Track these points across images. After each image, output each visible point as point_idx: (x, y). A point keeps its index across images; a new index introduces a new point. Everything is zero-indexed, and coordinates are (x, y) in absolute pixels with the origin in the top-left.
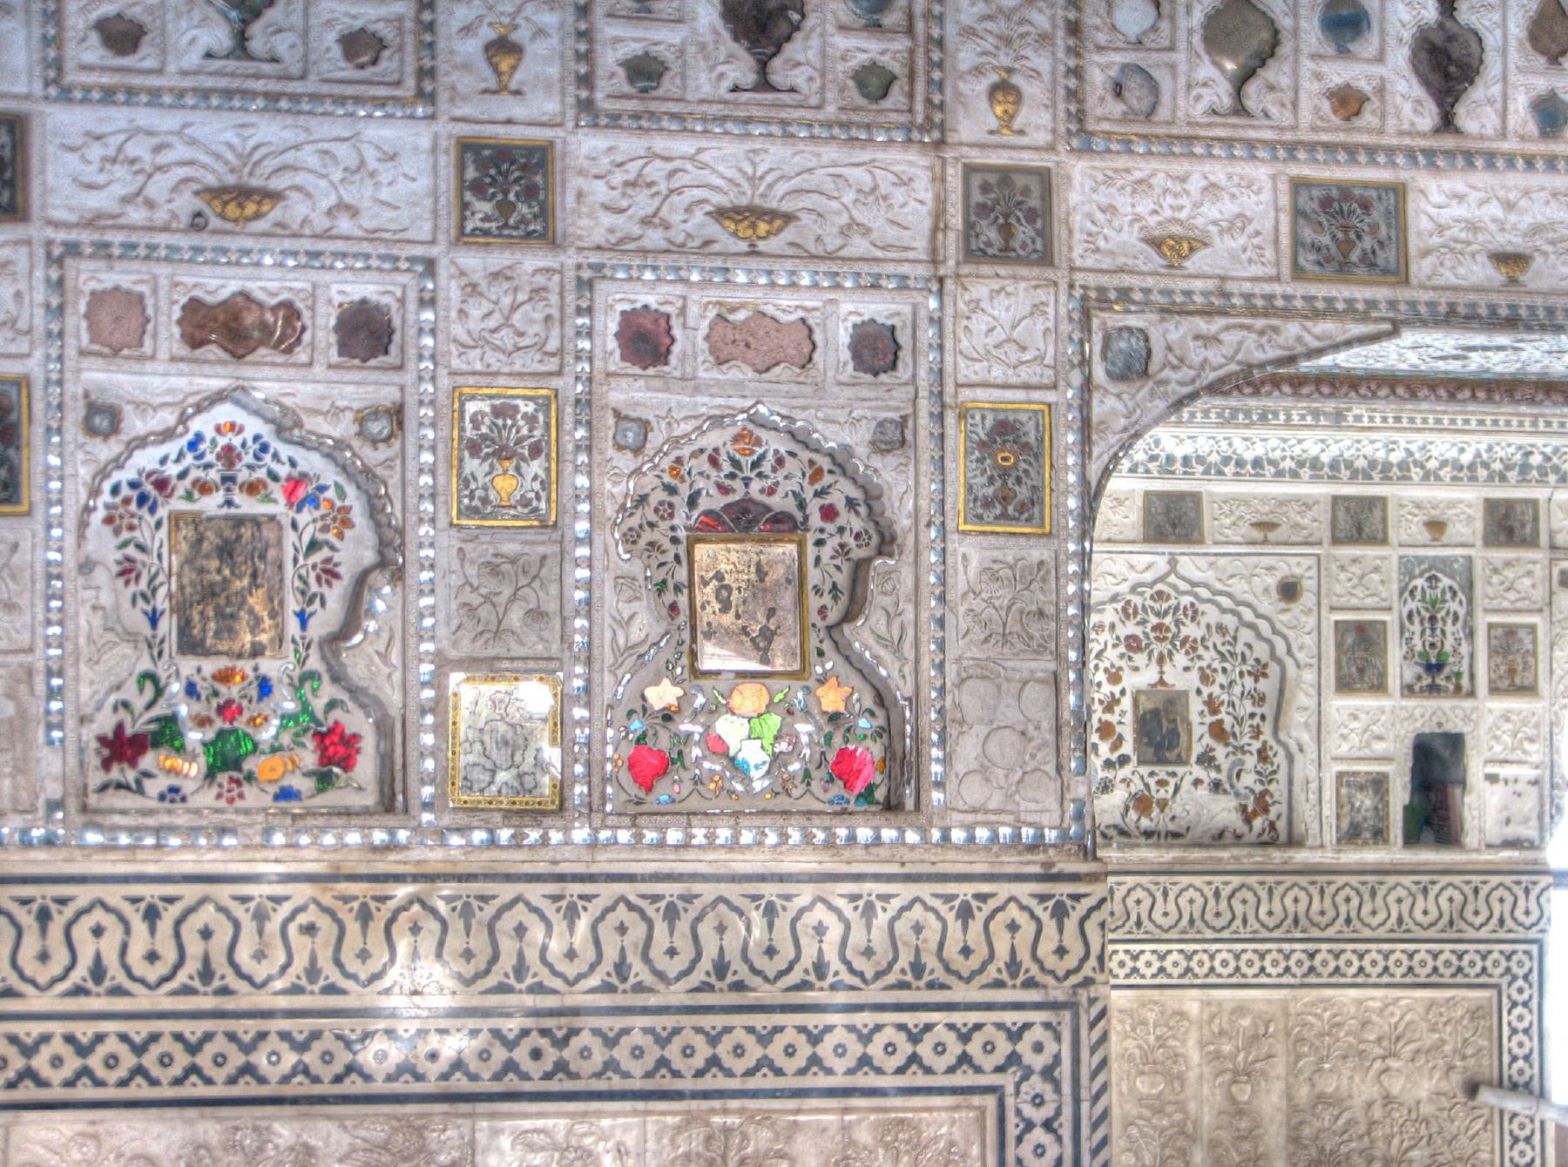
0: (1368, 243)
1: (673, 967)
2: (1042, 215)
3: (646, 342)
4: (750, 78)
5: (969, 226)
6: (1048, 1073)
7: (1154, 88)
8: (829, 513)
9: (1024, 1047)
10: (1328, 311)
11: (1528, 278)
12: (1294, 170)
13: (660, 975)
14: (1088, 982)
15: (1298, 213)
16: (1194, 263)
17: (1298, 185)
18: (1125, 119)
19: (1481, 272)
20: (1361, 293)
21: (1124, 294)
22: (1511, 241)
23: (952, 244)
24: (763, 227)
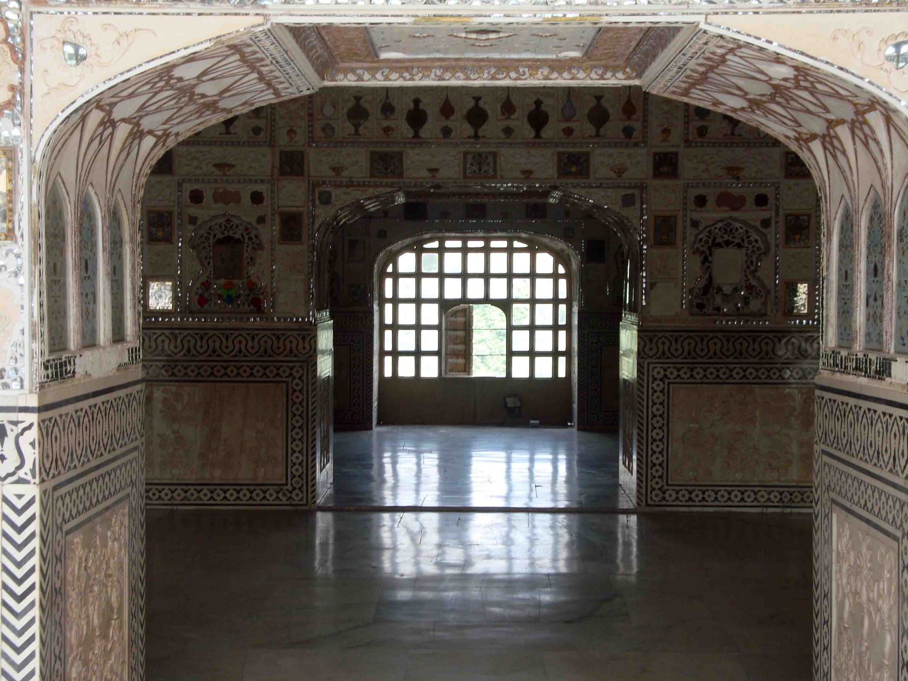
0: (392, 167)
1: (202, 351)
2: (301, 164)
3: (196, 197)
4: (225, 131)
5: (281, 166)
6: (300, 378)
7: (333, 129)
8: (250, 239)
9: (294, 371)
10: (381, 186)
11: (438, 175)
12: (372, 149)
13: (199, 353)
14: (311, 356)
15: (373, 161)
16: (344, 174)
17: (372, 153)
18: (325, 137)
19: (425, 174)
20: (390, 180)
21: (324, 183)
22: (434, 166)
23: (276, 171)
24: (227, 169)
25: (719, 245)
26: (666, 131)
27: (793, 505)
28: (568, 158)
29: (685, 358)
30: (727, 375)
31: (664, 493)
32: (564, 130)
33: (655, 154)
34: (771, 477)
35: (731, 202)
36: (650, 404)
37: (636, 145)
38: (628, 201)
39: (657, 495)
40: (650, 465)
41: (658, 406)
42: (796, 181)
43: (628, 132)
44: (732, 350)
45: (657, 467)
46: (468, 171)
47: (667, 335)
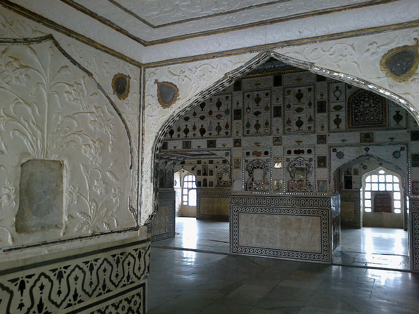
11: (176, 148)
19: (173, 148)
22: (175, 146)
25: (255, 168)
26: (237, 132)
27: (278, 256)
28: (210, 142)
29: (244, 204)
30: (256, 211)
31: (238, 248)
32: (209, 134)
33: (234, 139)
34: (271, 246)
35: (257, 154)
36: (233, 219)
37: (229, 137)
38: (227, 154)
39: (235, 249)
40: (233, 239)
41: (235, 220)
42: (277, 146)
43: (227, 133)
44: (258, 202)
45: (235, 240)
46: (184, 147)
47: (238, 197)
